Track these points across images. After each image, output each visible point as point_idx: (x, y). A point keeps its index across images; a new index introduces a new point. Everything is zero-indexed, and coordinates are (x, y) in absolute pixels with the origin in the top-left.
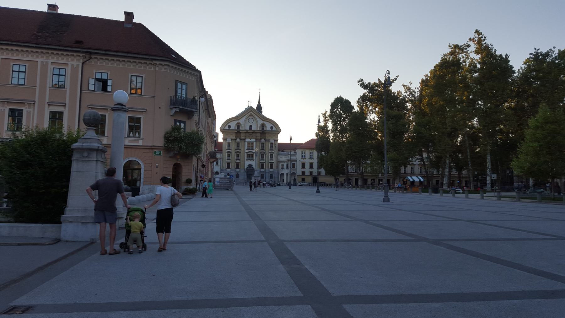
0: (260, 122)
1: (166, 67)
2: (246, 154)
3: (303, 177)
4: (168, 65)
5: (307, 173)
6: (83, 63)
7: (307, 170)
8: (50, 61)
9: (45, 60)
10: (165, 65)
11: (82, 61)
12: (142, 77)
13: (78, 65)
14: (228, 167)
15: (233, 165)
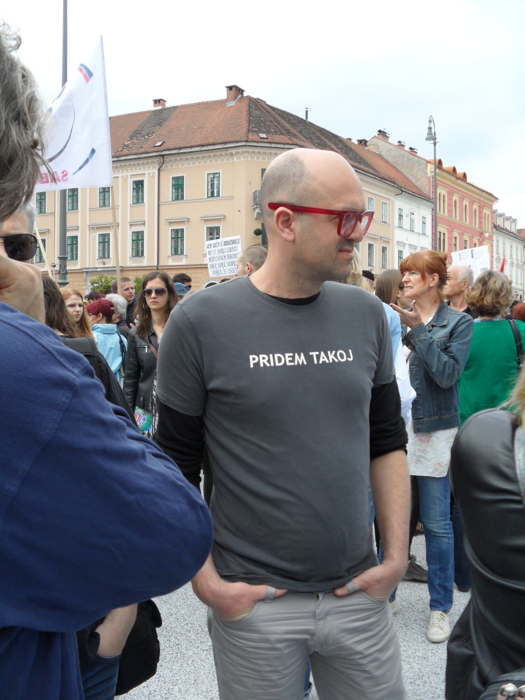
1: (246, 154)
4: (248, 152)
6: (159, 170)
8: (129, 174)
9: (124, 174)
10: (243, 152)
11: (157, 168)
12: (219, 173)
13: (154, 173)
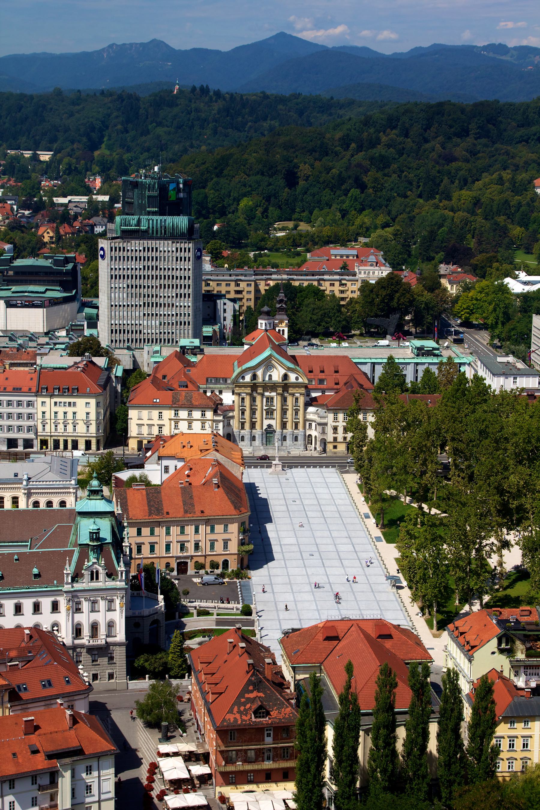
0: (283, 371)
2: (264, 412)
3: (335, 444)
5: (340, 439)
7: (340, 436)
14: (243, 428)
15: (247, 426)
